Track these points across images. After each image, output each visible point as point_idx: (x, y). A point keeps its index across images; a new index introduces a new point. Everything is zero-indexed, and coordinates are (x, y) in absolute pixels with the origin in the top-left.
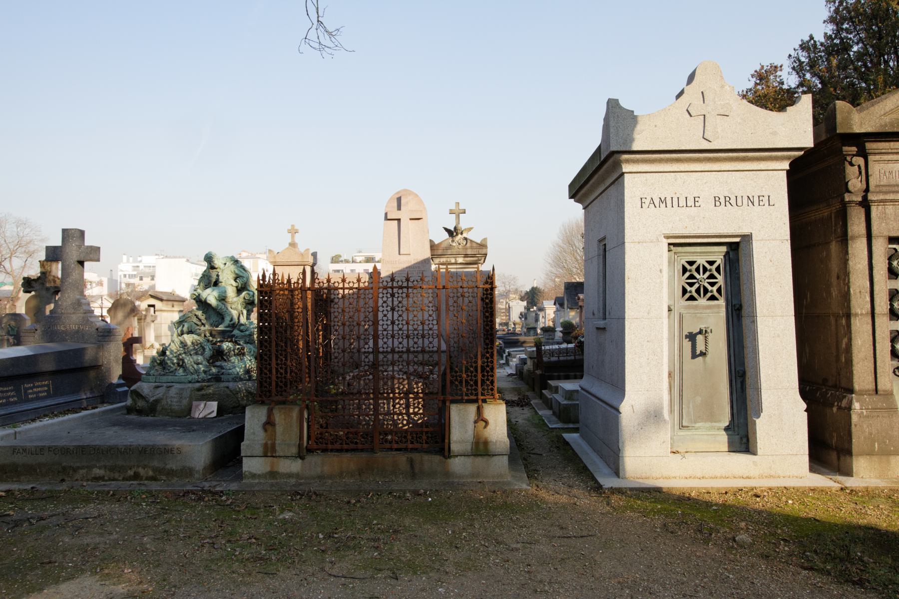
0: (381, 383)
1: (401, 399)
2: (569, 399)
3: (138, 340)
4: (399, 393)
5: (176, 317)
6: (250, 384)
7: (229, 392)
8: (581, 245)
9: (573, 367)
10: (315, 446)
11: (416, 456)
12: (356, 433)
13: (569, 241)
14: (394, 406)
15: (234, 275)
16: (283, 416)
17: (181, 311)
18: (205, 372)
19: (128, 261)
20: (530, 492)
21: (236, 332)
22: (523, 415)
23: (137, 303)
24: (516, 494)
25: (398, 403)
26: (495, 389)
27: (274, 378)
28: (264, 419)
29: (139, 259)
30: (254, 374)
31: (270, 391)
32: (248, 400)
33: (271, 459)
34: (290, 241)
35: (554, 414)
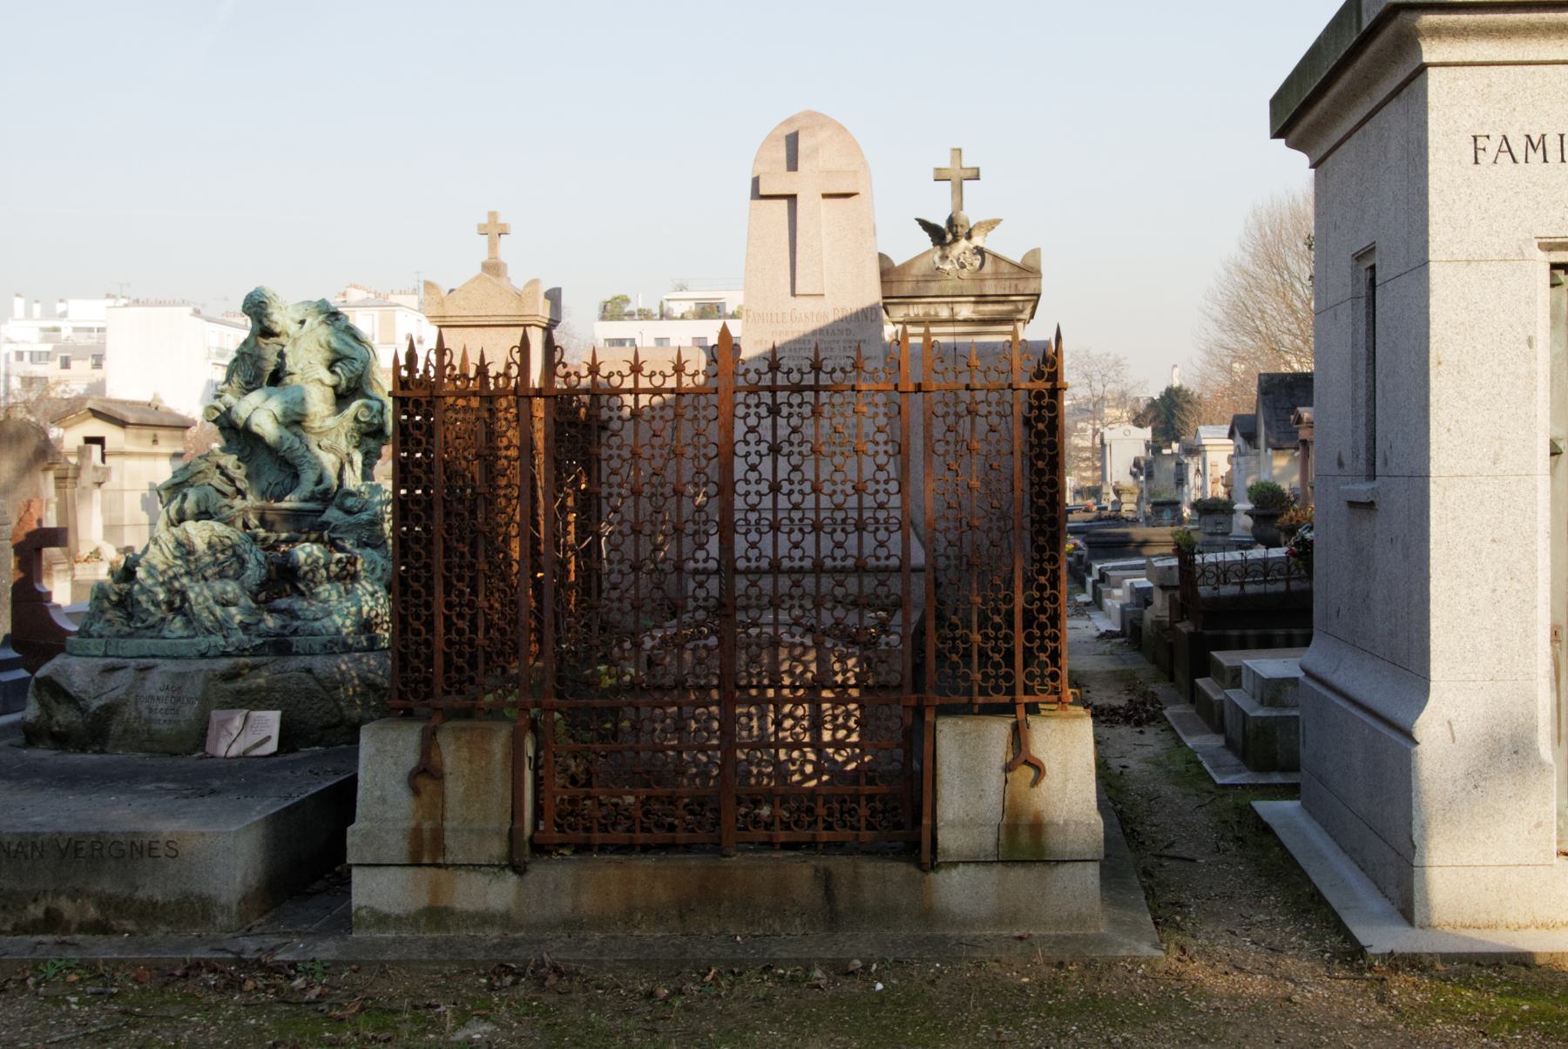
0: (743, 657)
1: (797, 702)
2: (1272, 703)
3: (57, 537)
4: (793, 688)
5: (163, 471)
6: (372, 661)
7: (312, 684)
8: (1306, 270)
9: (1282, 614)
10: (556, 837)
11: (840, 865)
12: (672, 800)
13: (1271, 257)
14: (778, 724)
15: (328, 355)
16: (465, 753)
17: (177, 456)
18: (245, 627)
19: (28, 315)
20: (1161, 966)
21: (333, 514)
22: (1141, 749)
23: (54, 433)
24: (1120, 972)
25: (791, 715)
26: (1064, 674)
27: (439, 643)
28: (411, 759)
29: (60, 308)
30: (384, 634)
31: (428, 682)
32: (365, 705)
33: (430, 871)
34: (485, 257)
35: (1229, 744)
